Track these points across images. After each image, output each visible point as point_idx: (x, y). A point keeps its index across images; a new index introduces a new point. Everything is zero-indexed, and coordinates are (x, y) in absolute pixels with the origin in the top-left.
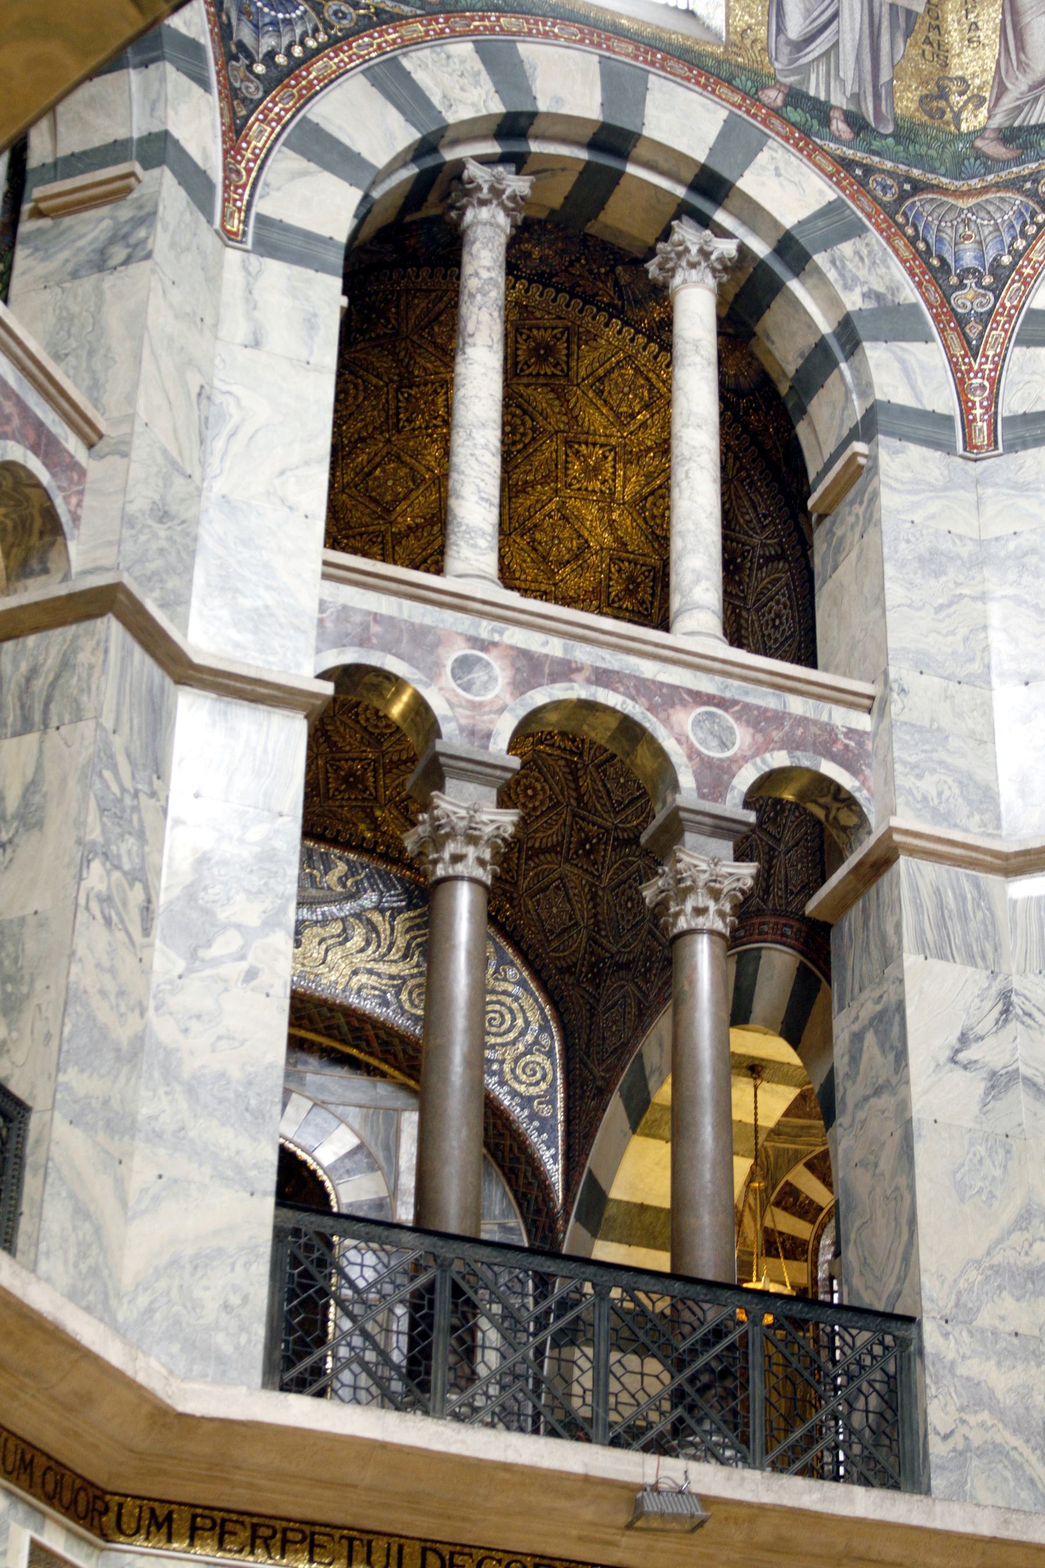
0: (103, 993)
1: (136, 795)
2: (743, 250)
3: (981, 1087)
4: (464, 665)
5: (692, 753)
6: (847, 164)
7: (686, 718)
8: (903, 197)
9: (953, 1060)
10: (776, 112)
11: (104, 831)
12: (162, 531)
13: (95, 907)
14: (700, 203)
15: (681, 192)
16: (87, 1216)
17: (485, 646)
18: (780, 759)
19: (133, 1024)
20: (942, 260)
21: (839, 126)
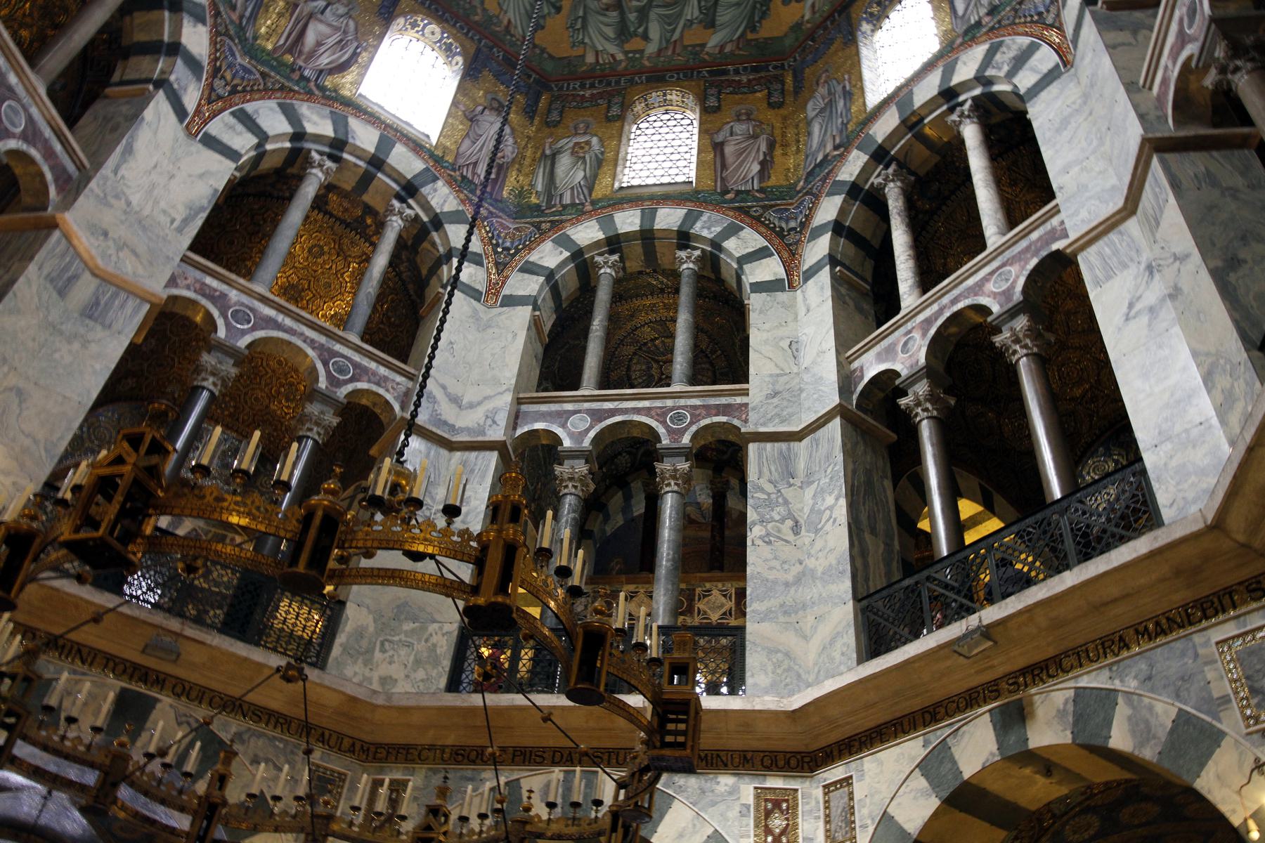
0: (771, 568)
1: (779, 491)
2: (974, 99)
3: (1145, 319)
4: (906, 344)
5: (995, 295)
6: (992, 29)
7: (990, 286)
8: (1016, 11)
9: (1127, 319)
10: (961, 44)
11: (758, 514)
12: (775, 401)
13: (759, 542)
14: (953, 103)
15: (945, 107)
16: (778, 651)
17: (910, 332)
18: (1034, 262)
19: (798, 568)
20: (1040, 14)
21: (987, 19)
